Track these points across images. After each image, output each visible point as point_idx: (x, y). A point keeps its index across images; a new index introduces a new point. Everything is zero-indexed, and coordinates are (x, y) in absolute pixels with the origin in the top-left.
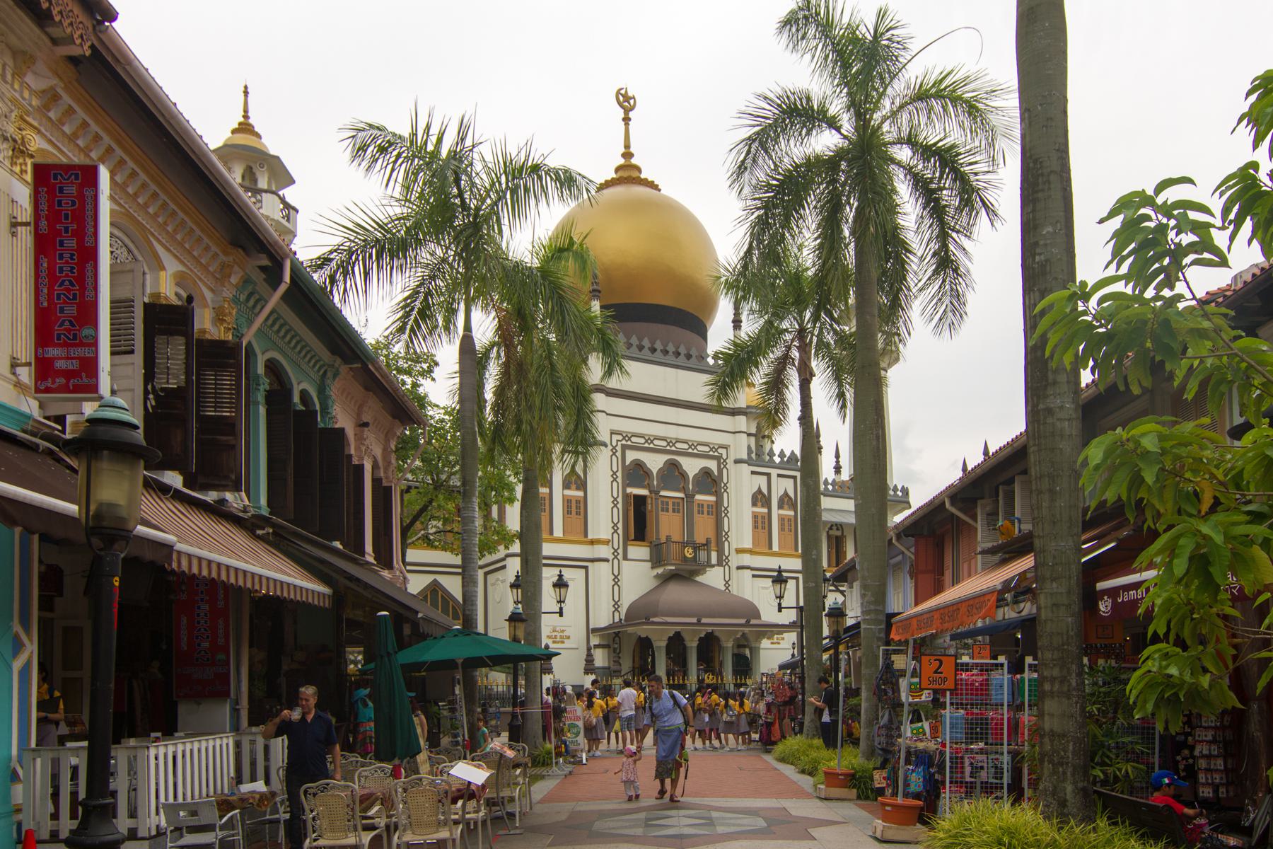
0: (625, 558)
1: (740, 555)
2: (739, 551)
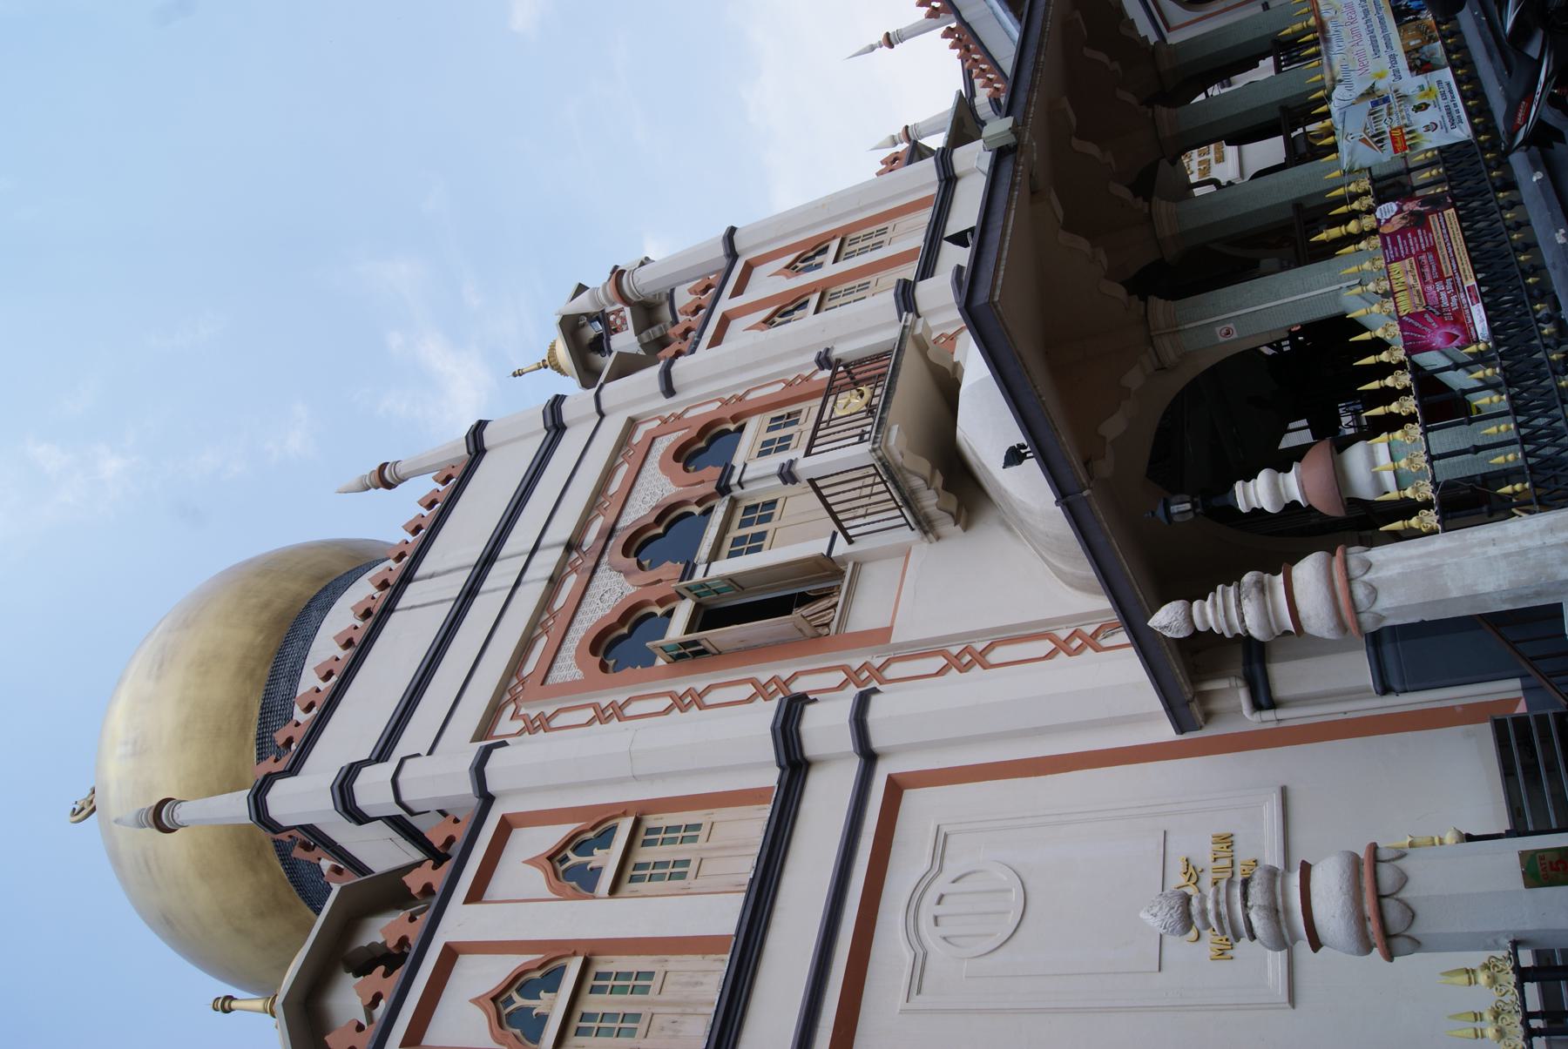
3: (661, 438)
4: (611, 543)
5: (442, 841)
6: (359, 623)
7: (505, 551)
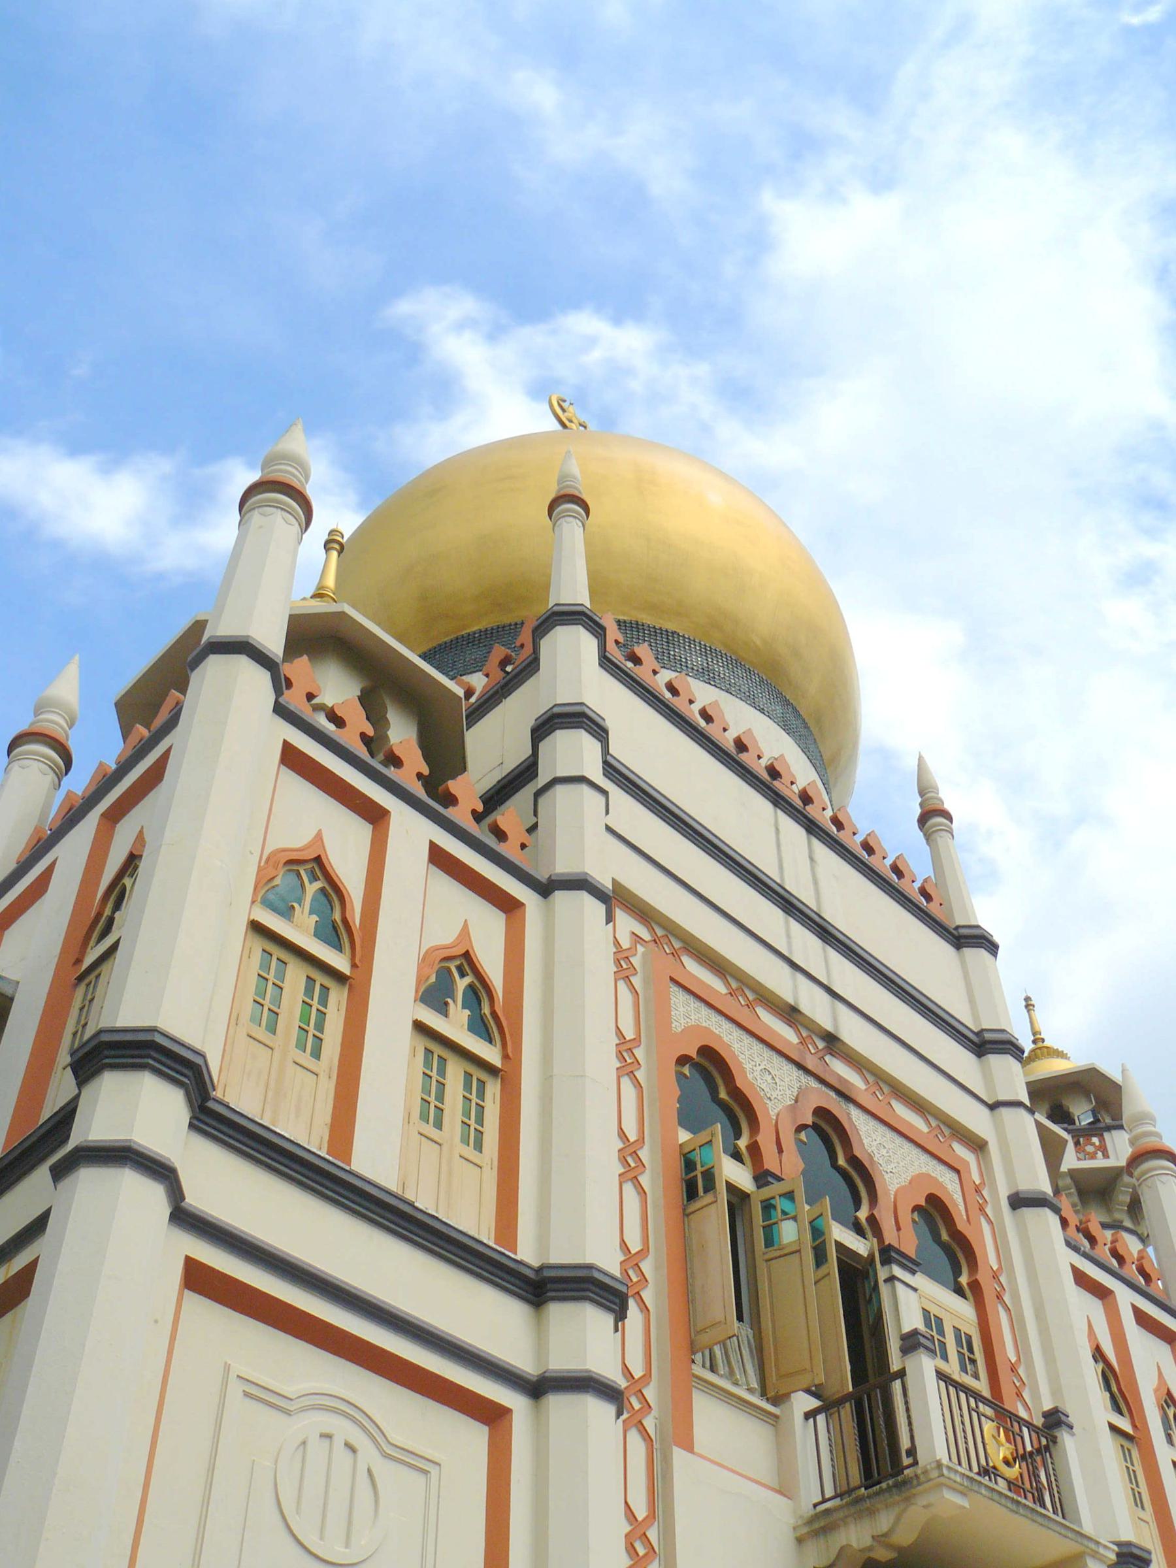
3: (958, 1182)
4: (833, 1094)
5: (503, 826)
6: (764, 762)
7: (834, 956)
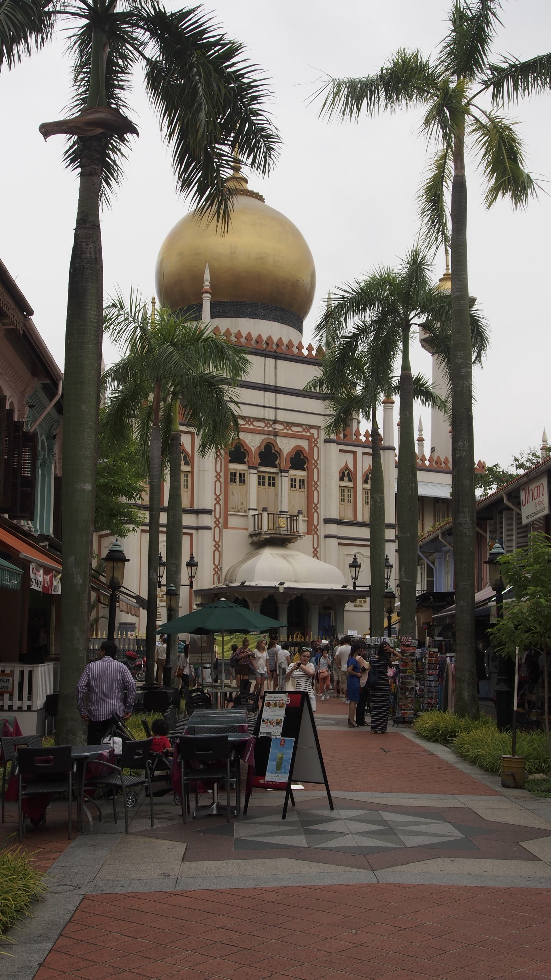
0: (226, 526)
1: (327, 525)
2: (327, 521)
4: (272, 437)
